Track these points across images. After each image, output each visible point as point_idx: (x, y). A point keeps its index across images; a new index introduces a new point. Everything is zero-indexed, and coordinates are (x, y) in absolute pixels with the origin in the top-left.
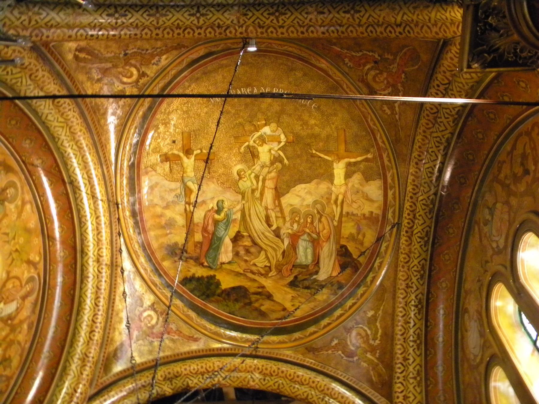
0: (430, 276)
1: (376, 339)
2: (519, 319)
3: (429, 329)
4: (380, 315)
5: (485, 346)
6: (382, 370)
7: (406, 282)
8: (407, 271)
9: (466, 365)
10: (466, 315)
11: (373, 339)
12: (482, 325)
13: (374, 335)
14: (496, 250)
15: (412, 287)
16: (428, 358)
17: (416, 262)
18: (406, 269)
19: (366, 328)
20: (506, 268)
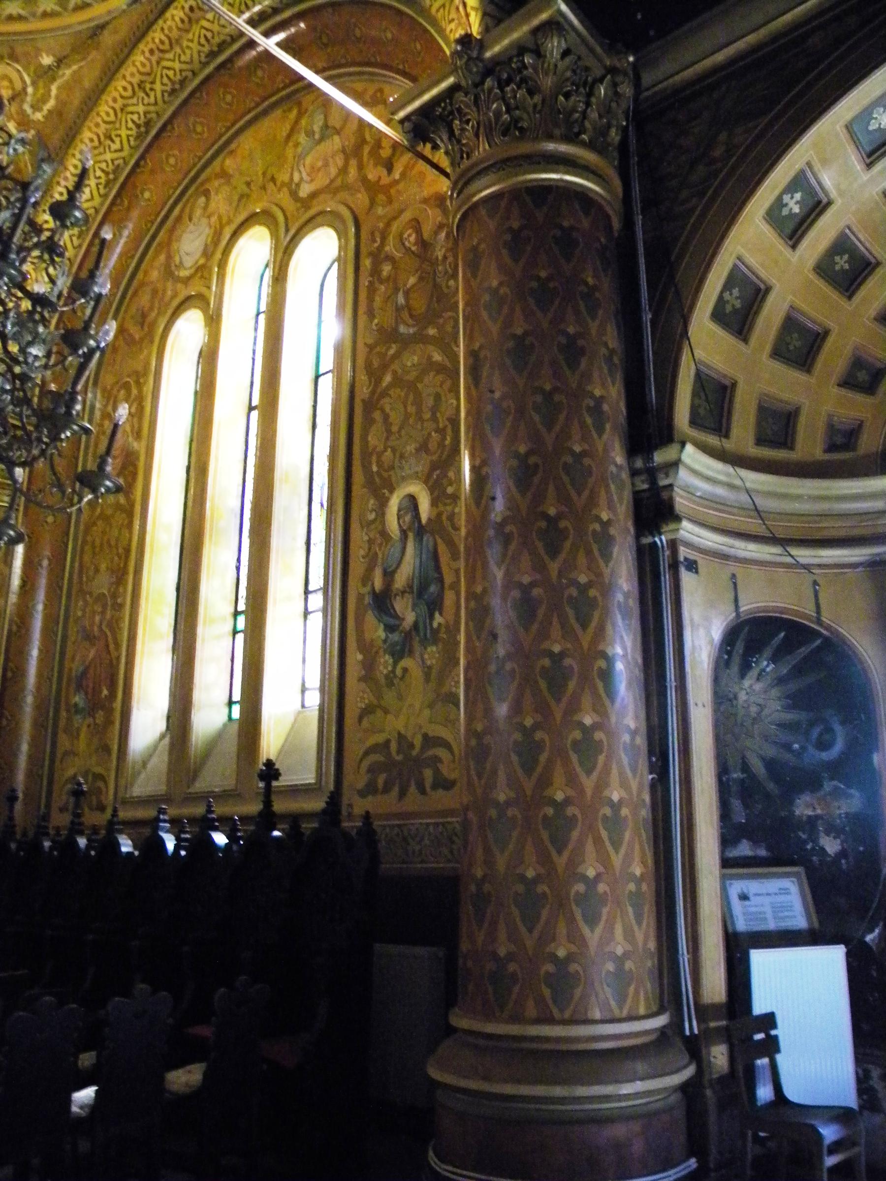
0: (185, 102)
1: (39, 109)
2: (261, 272)
3: (138, 170)
4: (65, 78)
5: (202, 271)
6: (26, 166)
7: (144, 78)
8: (154, 63)
9: (162, 258)
10: (202, 200)
11: (32, 107)
12: (216, 242)
13: (38, 101)
14: (294, 186)
15: (148, 95)
16: (115, 209)
17: (177, 65)
18: (154, 59)
19: (28, 80)
20: (287, 230)
